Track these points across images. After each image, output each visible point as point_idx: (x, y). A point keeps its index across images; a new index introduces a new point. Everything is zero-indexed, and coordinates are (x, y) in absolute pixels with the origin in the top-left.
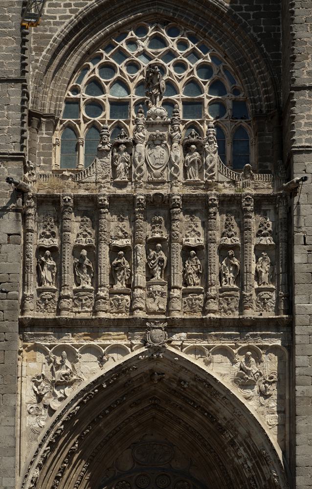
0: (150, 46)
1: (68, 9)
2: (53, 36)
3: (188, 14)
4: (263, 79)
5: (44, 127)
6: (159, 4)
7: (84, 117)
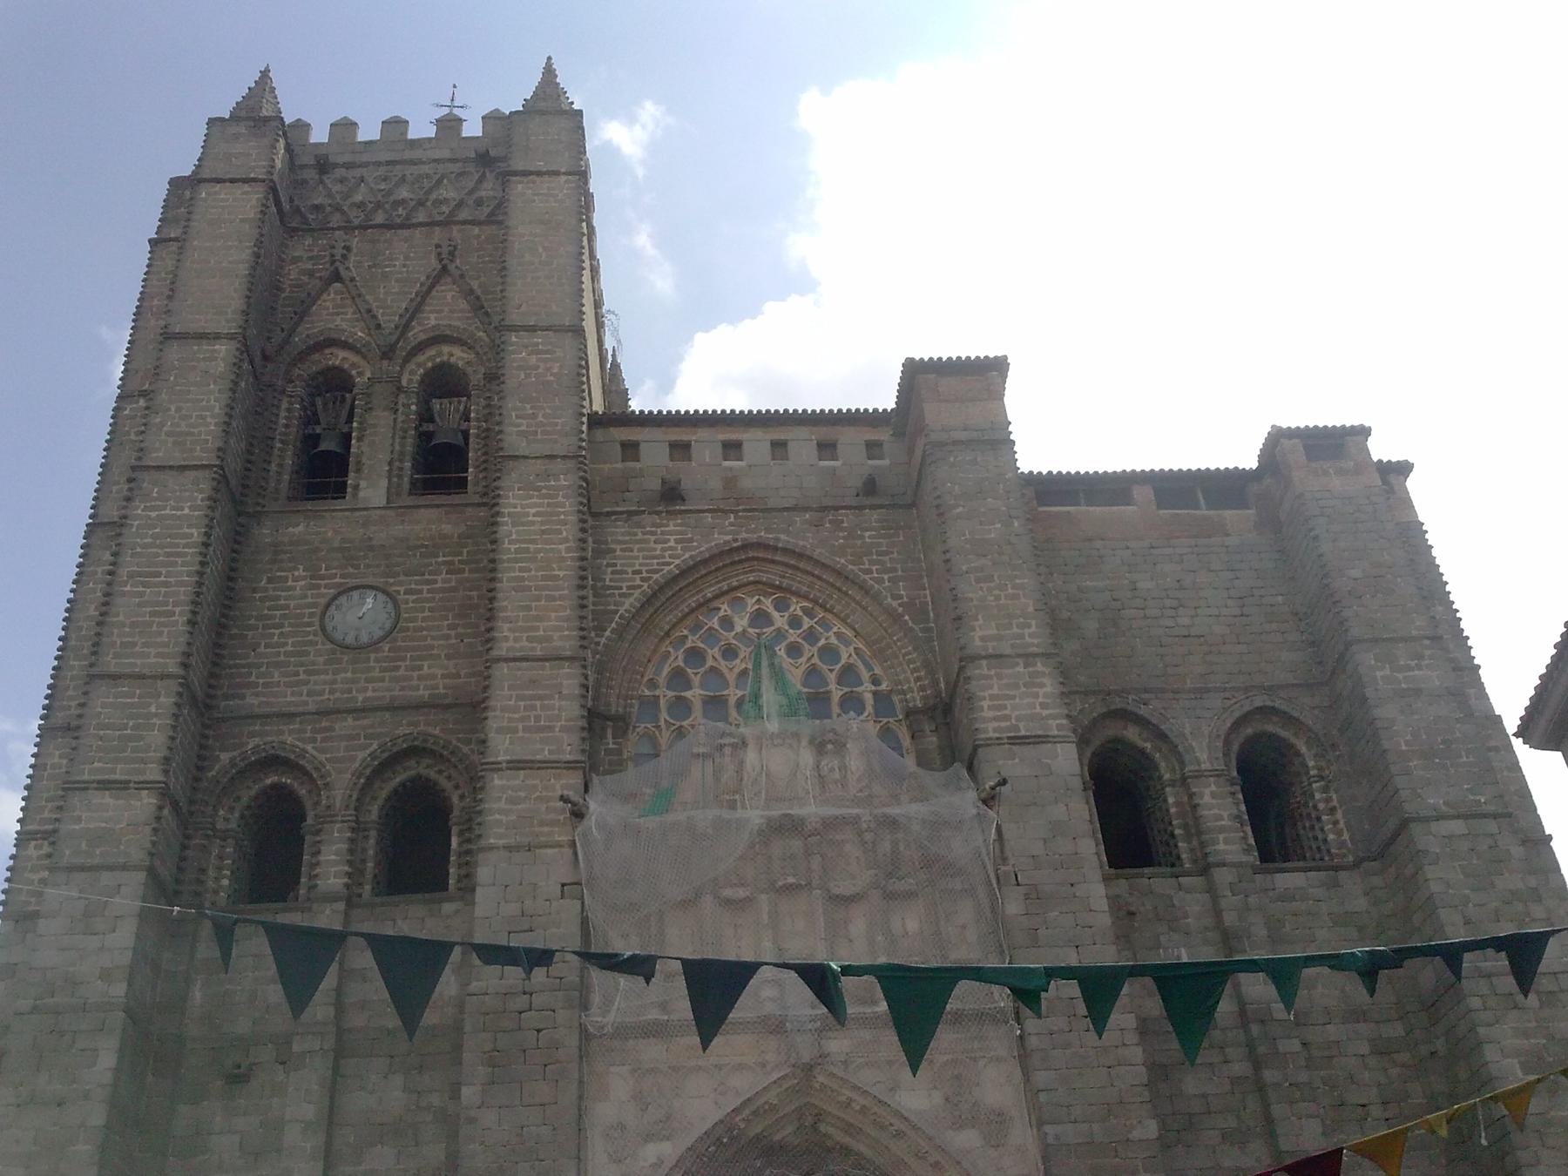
0: (750, 626)
1: (638, 577)
2: (618, 610)
3: (800, 582)
4: (910, 662)
5: (610, 735)
6: (759, 571)
7: (665, 720)
